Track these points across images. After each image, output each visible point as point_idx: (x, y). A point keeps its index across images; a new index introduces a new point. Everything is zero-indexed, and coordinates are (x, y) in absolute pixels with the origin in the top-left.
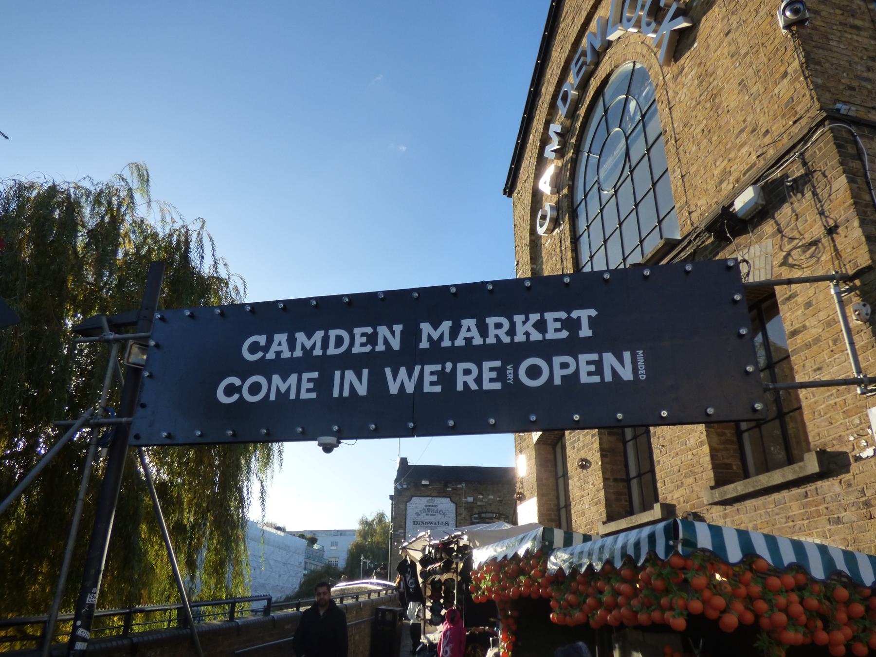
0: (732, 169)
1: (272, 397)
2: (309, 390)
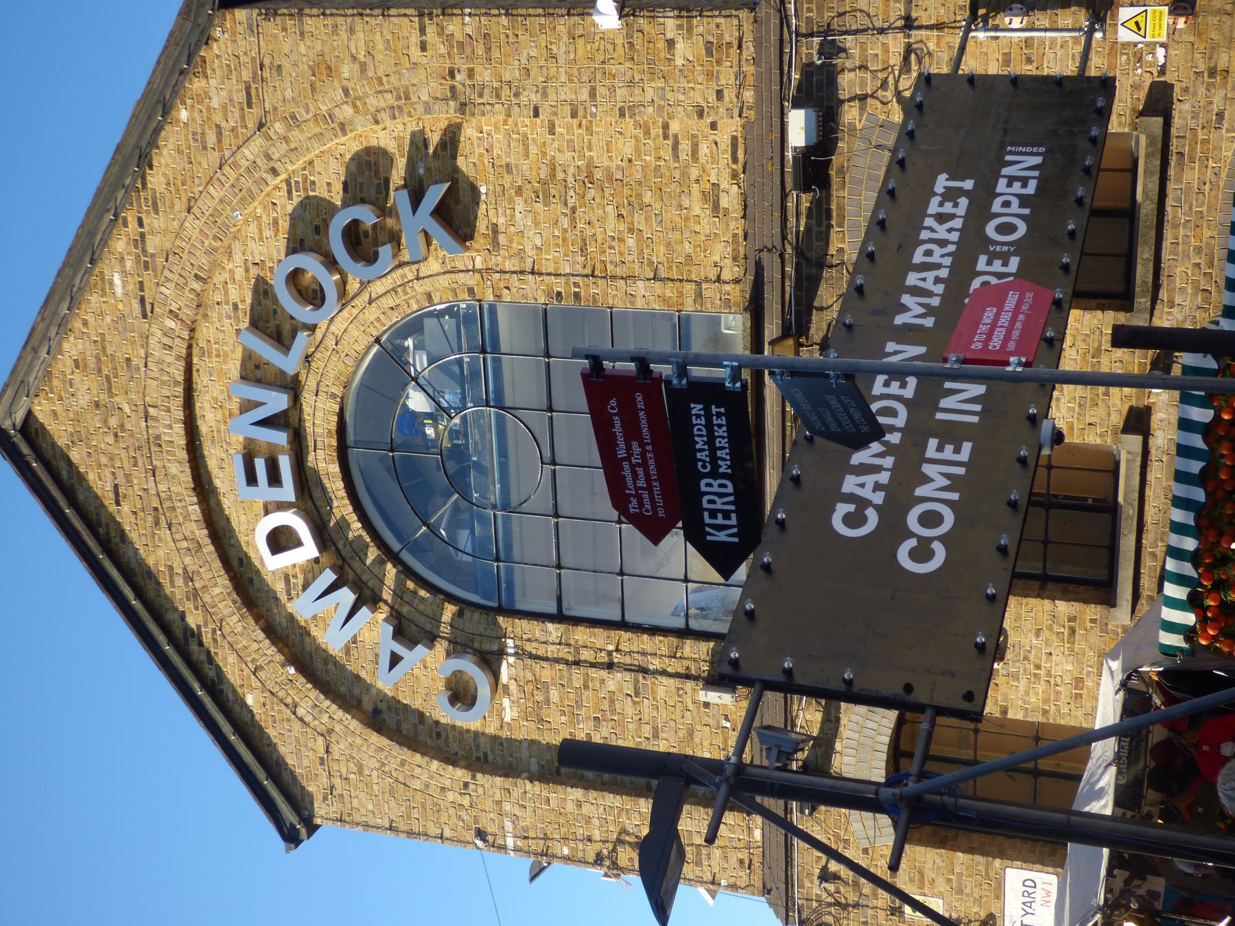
0: (713, 180)
1: (955, 496)
2: (957, 450)
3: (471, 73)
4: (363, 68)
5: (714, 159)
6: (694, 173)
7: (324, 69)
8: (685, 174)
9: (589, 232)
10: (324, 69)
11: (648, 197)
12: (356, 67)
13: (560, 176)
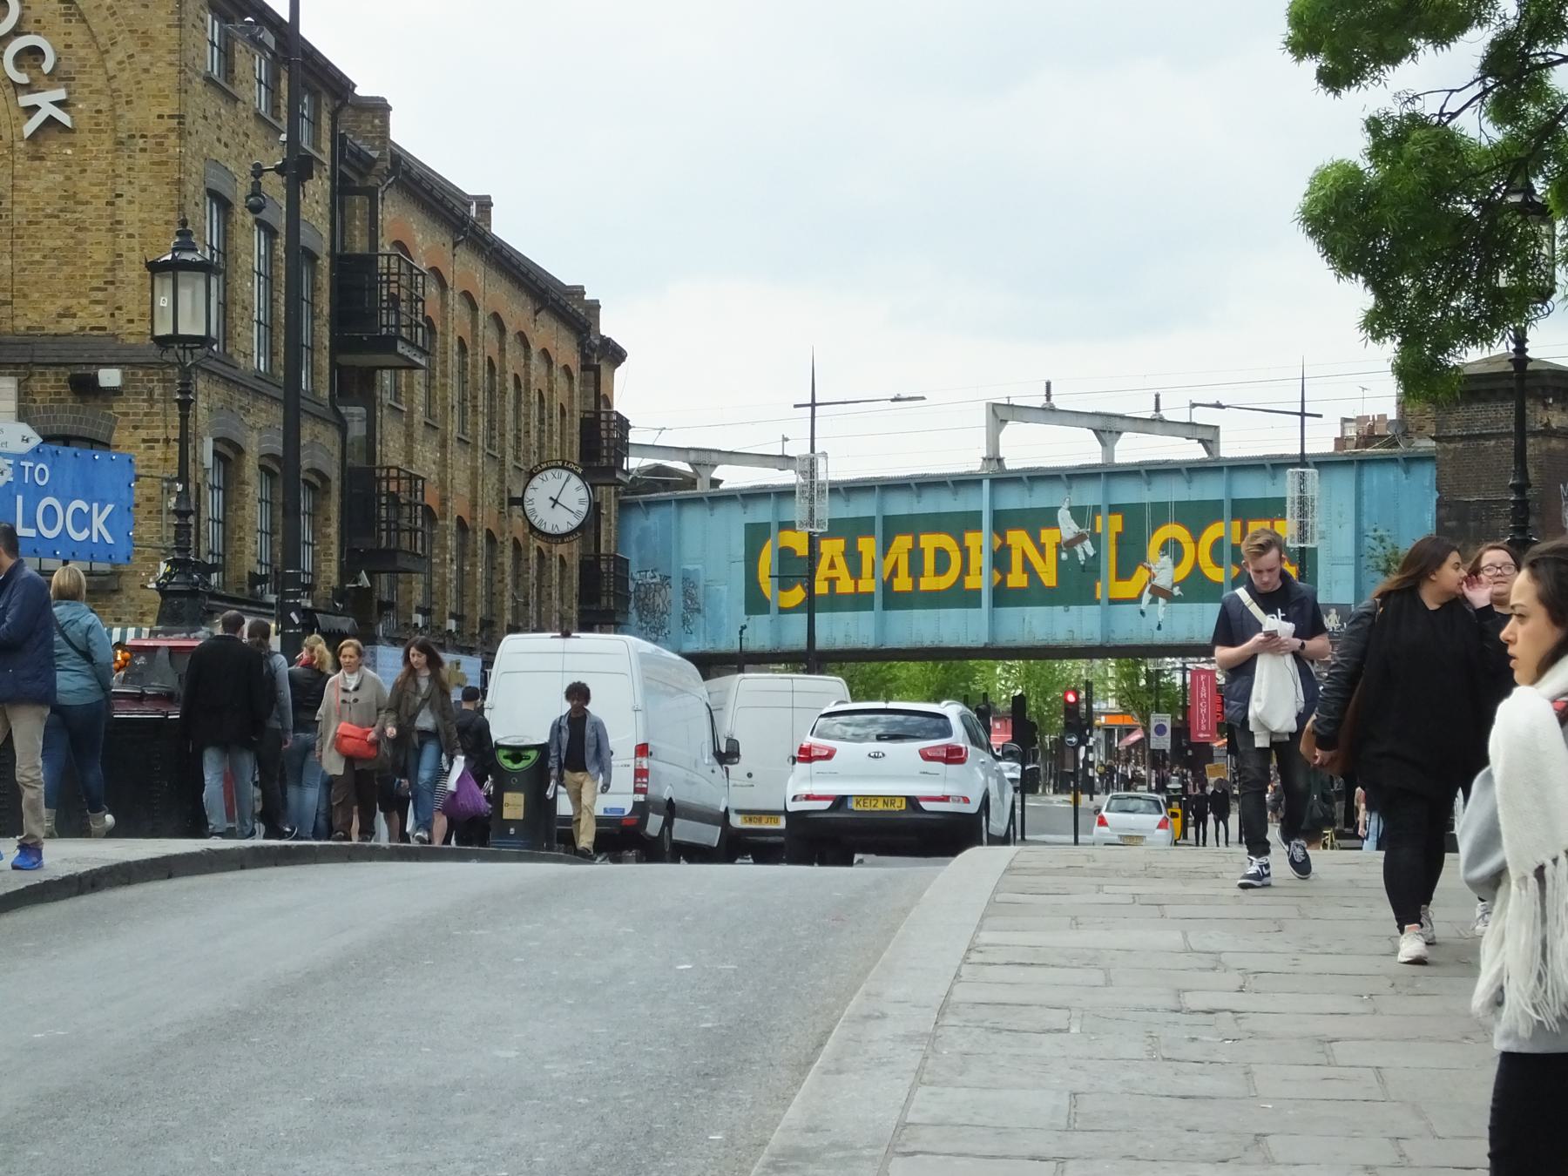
3: (143, 150)
4: (146, 71)
5: (93, 315)
6: (84, 301)
7: (146, 40)
8: (80, 295)
9: (42, 227)
10: (146, 40)
11: (67, 269)
12: (147, 66)
13: (80, 208)
